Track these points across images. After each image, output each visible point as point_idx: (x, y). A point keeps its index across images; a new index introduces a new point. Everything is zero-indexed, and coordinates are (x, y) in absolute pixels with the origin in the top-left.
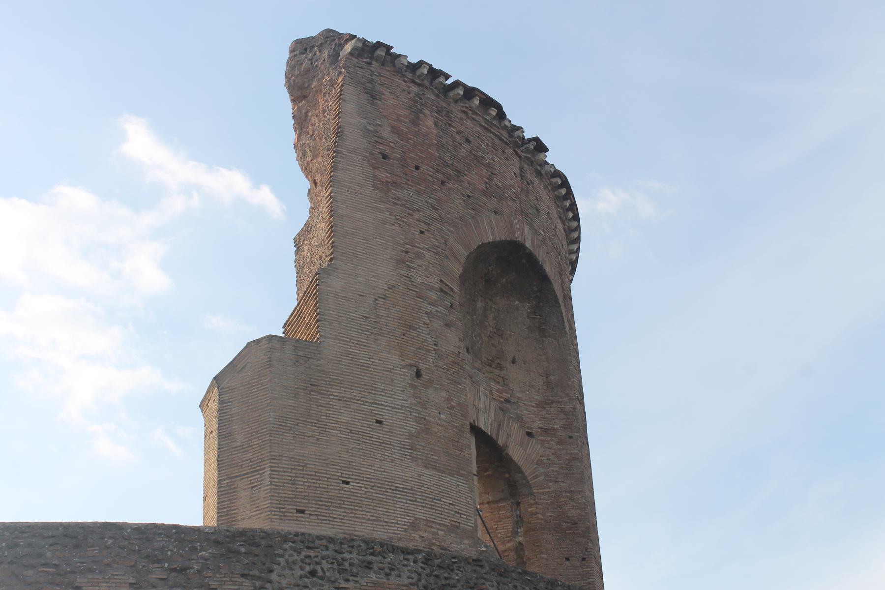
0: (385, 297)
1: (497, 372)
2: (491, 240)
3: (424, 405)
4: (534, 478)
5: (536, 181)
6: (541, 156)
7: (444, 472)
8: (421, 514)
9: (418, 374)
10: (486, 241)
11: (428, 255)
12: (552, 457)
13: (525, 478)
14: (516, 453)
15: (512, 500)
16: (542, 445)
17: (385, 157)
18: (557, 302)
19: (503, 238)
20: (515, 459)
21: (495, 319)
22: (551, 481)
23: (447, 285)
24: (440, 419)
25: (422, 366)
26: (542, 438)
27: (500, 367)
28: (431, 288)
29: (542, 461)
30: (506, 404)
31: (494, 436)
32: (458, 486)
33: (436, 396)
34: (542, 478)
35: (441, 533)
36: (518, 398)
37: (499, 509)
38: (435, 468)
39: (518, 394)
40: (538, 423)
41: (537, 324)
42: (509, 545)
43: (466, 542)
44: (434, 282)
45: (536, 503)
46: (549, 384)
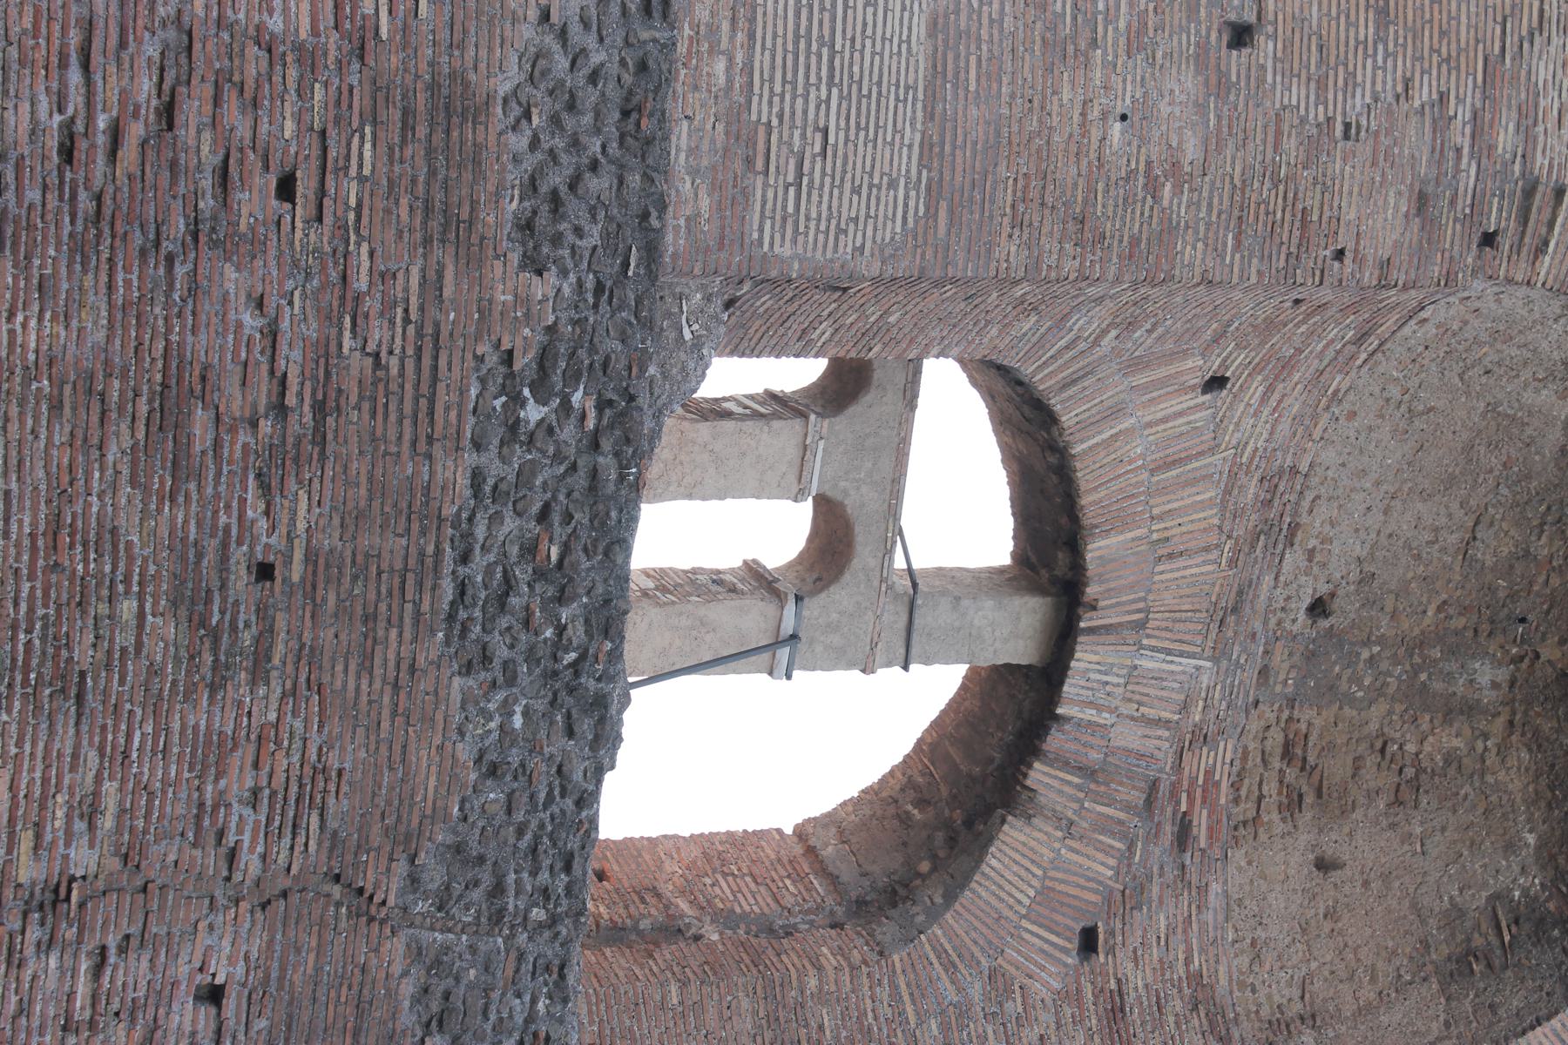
1: (1271, 788)
3: (1136, 41)
4: (941, 953)
7: (930, 116)
9: (1241, 35)
12: (1031, 1034)
13: (934, 915)
14: (1018, 857)
15: (840, 911)
16: (1062, 996)
20: (994, 861)
21: (1447, 762)
22: (945, 1028)
23: (1551, 225)
24: (1104, 116)
25: (1265, 48)
26: (1088, 991)
27: (1293, 803)
29: (1008, 991)
30: (1172, 821)
31: (1055, 741)
32: (893, 185)
34: (952, 995)
35: (720, 66)
36: (1203, 890)
37: (799, 878)
38: (937, 71)
39: (1215, 888)
40: (1137, 980)
41: (1478, 941)
42: (683, 905)
43: (705, 203)
45: (853, 968)
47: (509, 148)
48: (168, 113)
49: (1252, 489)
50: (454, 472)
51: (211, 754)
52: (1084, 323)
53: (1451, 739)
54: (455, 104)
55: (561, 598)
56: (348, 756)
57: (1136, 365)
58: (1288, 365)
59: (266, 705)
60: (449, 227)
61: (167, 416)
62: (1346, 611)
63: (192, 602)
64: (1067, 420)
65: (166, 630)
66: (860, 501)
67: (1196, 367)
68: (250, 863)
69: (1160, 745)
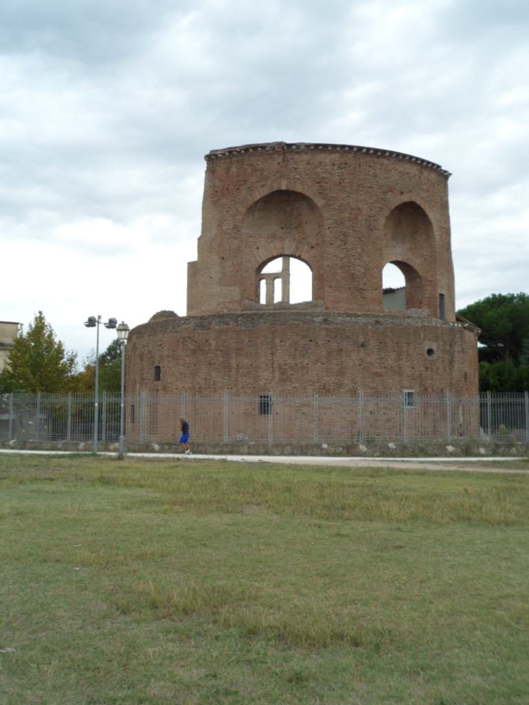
0: (214, 239)
2: (259, 198)
3: (224, 268)
5: (296, 156)
6: (294, 147)
8: (221, 300)
9: (223, 258)
10: (256, 200)
11: (228, 218)
17: (217, 192)
18: (311, 199)
19: (265, 194)
25: (224, 256)
27: (302, 227)
28: (228, 230)
46: (319, 226)
48: (220, 351)
49: (270, 240)
52: (250, 265)
54: (220, 332)
55: (254, 318)
56: (263, 334)
57: (255, 257)
58: (255, 242)
61: (239, 350)
64: (261, 261)
65: (253, 348)
66: (273, 278)
67: (255, 251)
68: (271, 340)
69: (295, 243)
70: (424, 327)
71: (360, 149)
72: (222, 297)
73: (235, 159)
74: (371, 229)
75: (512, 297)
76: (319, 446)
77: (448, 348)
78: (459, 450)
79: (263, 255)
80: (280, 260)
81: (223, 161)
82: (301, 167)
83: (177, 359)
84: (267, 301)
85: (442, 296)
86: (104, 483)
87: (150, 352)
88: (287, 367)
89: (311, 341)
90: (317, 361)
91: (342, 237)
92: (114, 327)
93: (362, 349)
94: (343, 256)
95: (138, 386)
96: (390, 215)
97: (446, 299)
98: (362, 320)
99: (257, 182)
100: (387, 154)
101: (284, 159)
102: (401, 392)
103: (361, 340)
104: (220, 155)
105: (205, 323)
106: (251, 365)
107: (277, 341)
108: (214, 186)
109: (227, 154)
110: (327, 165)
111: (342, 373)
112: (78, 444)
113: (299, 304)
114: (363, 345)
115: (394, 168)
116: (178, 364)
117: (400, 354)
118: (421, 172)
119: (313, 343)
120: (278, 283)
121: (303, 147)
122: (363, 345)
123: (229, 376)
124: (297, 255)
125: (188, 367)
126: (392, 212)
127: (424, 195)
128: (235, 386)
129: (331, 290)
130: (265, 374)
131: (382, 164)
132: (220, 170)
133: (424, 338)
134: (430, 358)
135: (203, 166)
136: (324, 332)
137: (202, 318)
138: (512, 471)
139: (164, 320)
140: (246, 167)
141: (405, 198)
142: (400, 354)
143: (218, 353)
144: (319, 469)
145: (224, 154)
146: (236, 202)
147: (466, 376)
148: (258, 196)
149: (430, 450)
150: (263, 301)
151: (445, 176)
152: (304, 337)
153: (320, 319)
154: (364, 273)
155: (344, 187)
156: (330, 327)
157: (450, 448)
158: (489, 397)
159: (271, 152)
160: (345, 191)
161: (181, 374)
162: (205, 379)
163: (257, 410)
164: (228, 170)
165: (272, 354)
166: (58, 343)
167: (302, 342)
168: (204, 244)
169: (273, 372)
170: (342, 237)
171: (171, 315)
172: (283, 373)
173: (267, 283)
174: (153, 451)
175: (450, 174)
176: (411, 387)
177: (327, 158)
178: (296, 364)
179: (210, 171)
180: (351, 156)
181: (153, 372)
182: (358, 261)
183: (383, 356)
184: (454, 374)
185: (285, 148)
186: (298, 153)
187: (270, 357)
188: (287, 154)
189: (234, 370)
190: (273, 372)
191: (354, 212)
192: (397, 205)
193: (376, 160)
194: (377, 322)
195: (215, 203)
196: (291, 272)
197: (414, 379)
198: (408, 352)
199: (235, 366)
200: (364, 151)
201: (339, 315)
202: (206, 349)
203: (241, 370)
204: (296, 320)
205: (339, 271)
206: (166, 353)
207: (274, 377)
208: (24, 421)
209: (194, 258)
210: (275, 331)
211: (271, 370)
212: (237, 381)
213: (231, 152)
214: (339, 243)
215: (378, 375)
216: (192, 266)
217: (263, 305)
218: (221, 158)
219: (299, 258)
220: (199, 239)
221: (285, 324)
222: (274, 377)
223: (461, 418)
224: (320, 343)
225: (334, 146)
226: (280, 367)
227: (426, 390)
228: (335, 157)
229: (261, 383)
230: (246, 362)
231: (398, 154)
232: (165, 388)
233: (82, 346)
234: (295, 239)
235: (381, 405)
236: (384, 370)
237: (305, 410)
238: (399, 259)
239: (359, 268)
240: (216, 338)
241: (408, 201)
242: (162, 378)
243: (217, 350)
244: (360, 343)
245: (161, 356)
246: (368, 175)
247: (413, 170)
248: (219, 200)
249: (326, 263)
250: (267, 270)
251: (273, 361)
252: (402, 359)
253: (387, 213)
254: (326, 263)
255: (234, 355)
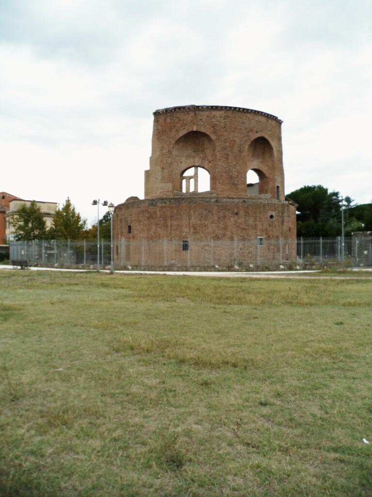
2: (181, 135)
5: (201, 113)
6: (200, 107)
8: (162, 191)
10: (180, 136)
27: (204, 151)
28: (166, 153)
33: (165, 171)
44: (167, 151)
46: (214, 151)
47: (163, 204)
50: (174, 205)
51: (184, 213)
52: (177, 171)
53: (201, 143)
54: (161, 207)
59: (182, 212)
60: (165, 207)
62: (194, 150)
63: (178, 215)
67: (180, 163)
70: (268, 204)
71: (235, 108)
72: (163, 189)
73: (169, 114)
74: (240, 151)
75: (315, 187)
76: (214, 267)
77: (281, 214)
78: (286, 268)
79: (184, 166)
80: (193, 168)
81: (162, 116)
82: (204, 118)
83: (140, 222)
84: (186, 191)
85: (278, 187)
86: (103, 286)
87: (126, 218)
88: (197, 226)
89: (209, 212)
90: (212, 222)
91: (226, 156)
92: (107, 205)
93: (236, 216)
94: (226, 166)
95: (119, 236)
96: (251, 144)
97: (280, 189)
98: (236, 201)
99: (181, 127)
100: (249, 111)
101: (195, 115)
102: (256, 238)
103: (236, 211)
104: (161, 113)
105: (154, 203)
106: (178, 225)
107: (192, 212)
108: (158, 129)
109: (165, 112)
110: (217, 117)
111: (225, 229)
112: (89, 266)
113: (203, 193)
114: (237, 214)
115: (253, 119)
116: (140, 224)
117: (256, 218)
118: (268, 121)
119: (210, 213)
120: (192, 181)
121: (205, 107)
122: (237, 214)
123: (167, 231)
124: (202, 166)
125: (146, 226)
126: (252, 142)
127: (269, 133)
128: (170, 235)
129: (219, 184)
130: (186, 230)
131: (247, 117)
132: (161, 120)
133: (269, 210)
134: (272, 220)
135: (152, 118)
136: (216, 207)
137: (152, 200)
138: (313, 278)
139: (133, 202)
140: (175, 118)
141: (259, 135)
142: (256, 218)
143: (161, 218)
144: (214, 279)
145: (163, 112)
146: (170, 138)
147: (290, 229)
148: (182, 133)
149: (271, 268)
150: (184, 191)
151: (279, 122)
152: (205, 209)
153: (214, 200)
154: (238, 175)
155: (226, 129)
156: (219, 204)
157: (282, 267)
158: (302, 240)
159: (188, 110)
160: (227, 131)
161: (142, 230)
162: (154, 232)
163: (181, 249)
164: (165, 120)
165: (189, 219)
166: (78, 213)
167: (205, 212)
168: (152, 161)
169: (190, 228)
170: (226, 156)
171: (136, 198)
172: (195, 229)
173: (186, 181)
174: (128, 270)
175: (282, 122)
176: (262, 236)
177: (217, 113)
178: (202, 224)
179: (156, 121)
180: (231, 112)
181: (127, 229)
182: (234, 169)
183: (247, 219)
184: (284, 228)
185: (196, 108)
186: (202, 111)
187: (188, 221)
188: (197, 112)
189: (169, 227)
190: (190, 228)
191: (232, 143)
192: (254, 138)
193: (243, 114)
194: (244, 201)
195: (158, 138)
196: (198, 175)
197: (263, 231)
198: (260, 217)
199: (170, 225)
200: (238, 109)
201: (224, 198)
202: (155, 216)
203: (173, 228)
204: (201, 201)
205: (224, 174)
206: (134, 219)
207: (190, 231)
208: (62, 254)
209: (148, 168)
210: (191, 207)
211: (188, 227)
212: (171, 233)
213: (167, 111)
214: (224, 159)
215: (244, 229)
216: (148, 174)
217: (184, 193)
218: (161, 114)
219: (203, 167)
220: (150, 158)
221: (195, 203)
222: (190, 231)
223: (287, 251)
224: (214, 213)
225: (222, 107)
226: (193, 226)
227: (269, 236)
228: (222, 112)
229: (184, 234)
230: (175, 223)
231: (255, 111)
232: (133, 237)
233: (90, 216)
234: (200, 157)
235: (246, 245)
236: (247, 227)
237: (207, 248)
238: (256, 167)
239: (235, 173)
240: (160, 211)
241: (261, 137)
242: (132, 232)
243: (160, 217)
244: (235, 213)
245: (131, 221)
246: (239, 122)
247: (263, 119)
248: (161, 137)
249: (217, 170)
250: (185, 174)
251: (190, 223)
252: (257, 221)
253: (249, 143)
254: (217, 170)
255: (169, 219)
